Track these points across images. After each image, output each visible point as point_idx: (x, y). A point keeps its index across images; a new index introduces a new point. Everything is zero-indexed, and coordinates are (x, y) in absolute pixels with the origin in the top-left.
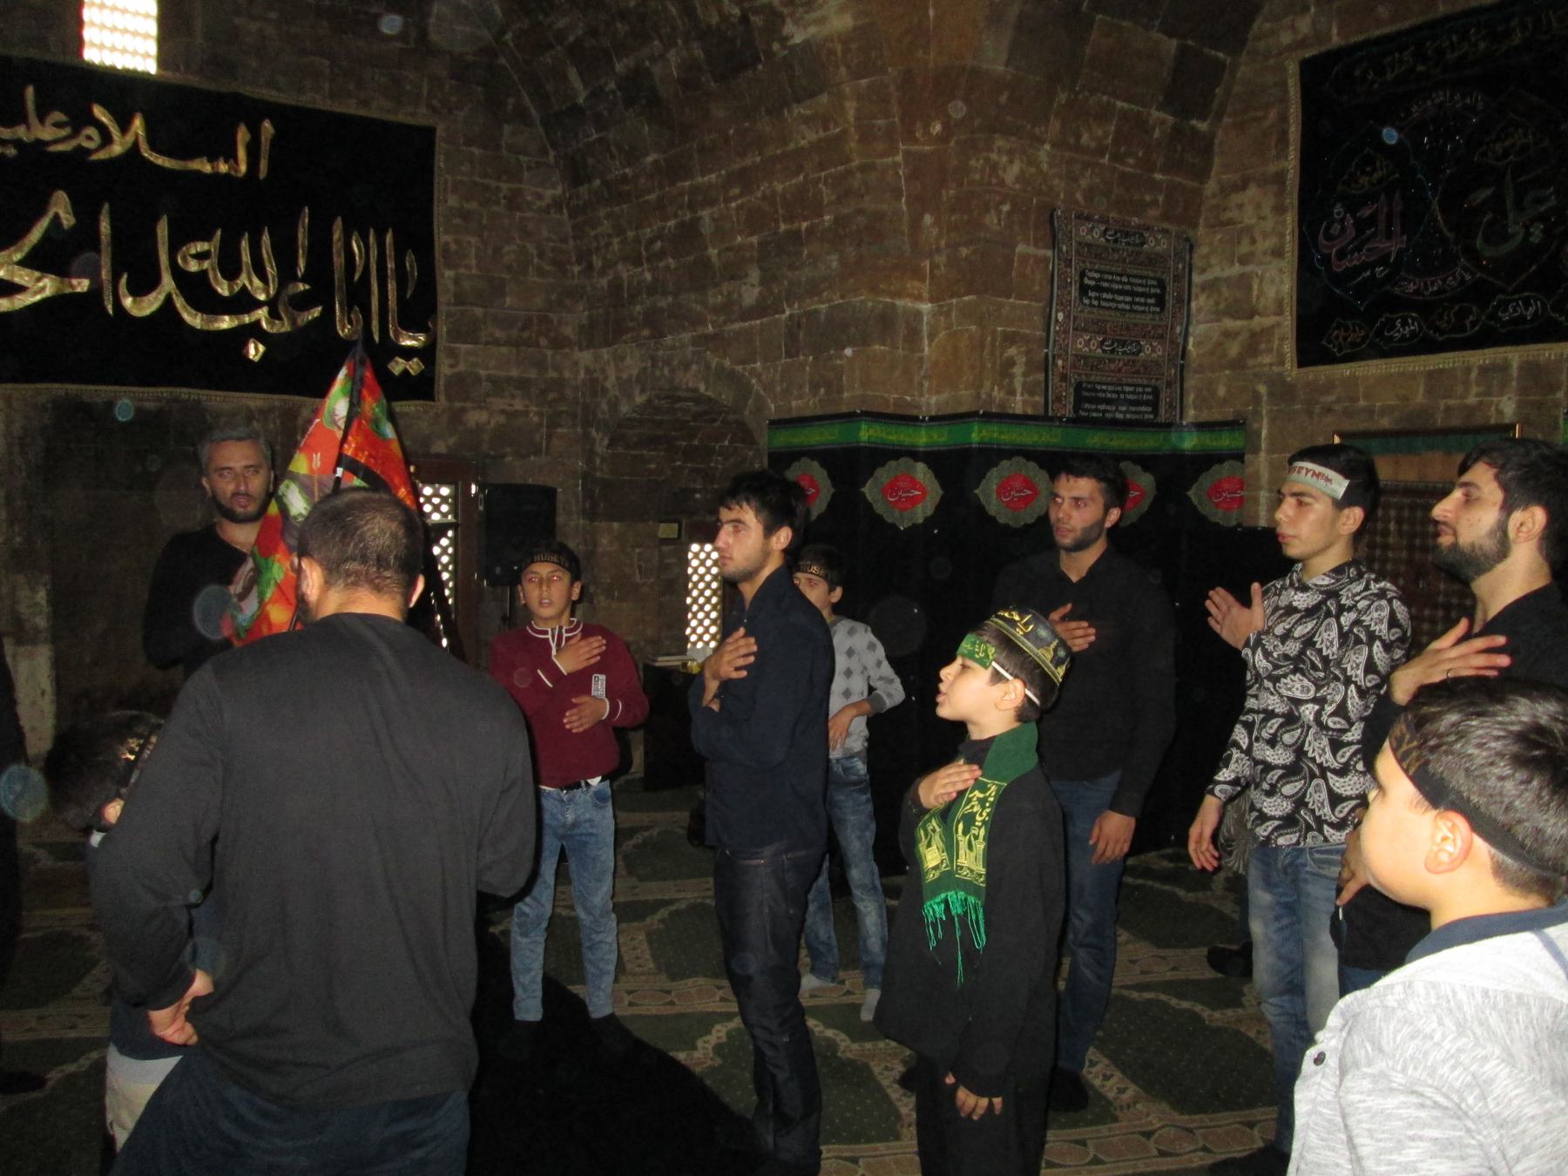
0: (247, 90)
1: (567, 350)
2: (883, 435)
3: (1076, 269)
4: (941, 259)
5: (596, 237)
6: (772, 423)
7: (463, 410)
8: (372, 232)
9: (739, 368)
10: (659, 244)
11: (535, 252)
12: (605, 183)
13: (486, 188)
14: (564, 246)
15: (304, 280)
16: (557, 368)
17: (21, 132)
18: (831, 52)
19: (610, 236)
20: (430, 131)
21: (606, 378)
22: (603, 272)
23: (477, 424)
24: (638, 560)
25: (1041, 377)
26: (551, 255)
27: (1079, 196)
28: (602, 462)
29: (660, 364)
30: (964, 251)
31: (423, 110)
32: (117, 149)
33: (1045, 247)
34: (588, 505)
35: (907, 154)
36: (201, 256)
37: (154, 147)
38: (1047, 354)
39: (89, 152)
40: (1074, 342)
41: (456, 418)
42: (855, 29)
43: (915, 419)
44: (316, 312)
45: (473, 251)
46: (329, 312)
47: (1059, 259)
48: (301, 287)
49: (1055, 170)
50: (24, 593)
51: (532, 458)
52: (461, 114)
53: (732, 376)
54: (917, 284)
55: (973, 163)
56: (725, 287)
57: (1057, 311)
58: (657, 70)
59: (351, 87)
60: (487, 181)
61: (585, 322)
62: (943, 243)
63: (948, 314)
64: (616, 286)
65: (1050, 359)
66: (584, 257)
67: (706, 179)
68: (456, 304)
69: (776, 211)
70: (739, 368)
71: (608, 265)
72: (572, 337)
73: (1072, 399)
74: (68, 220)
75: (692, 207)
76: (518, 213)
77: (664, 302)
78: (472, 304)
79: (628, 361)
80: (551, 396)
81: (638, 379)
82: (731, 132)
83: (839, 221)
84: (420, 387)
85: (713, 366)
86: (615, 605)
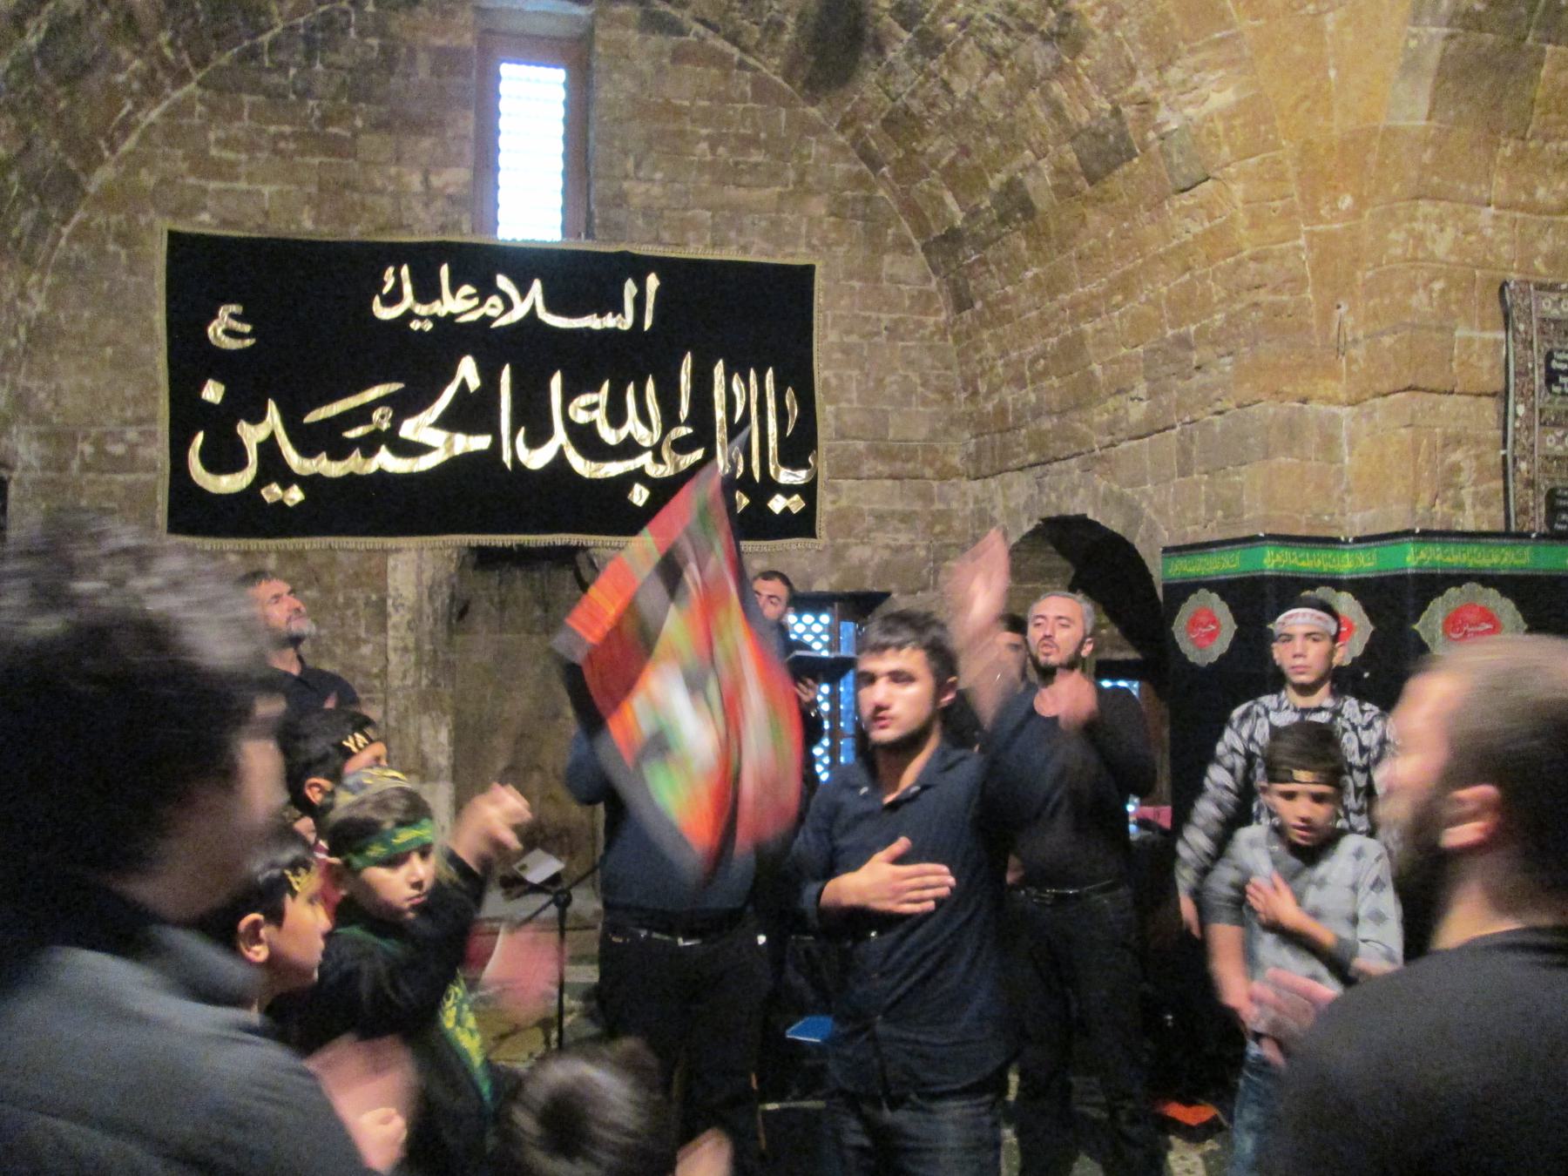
1: (954, 480)
2: (1295, 561)
3: (1539, 351)
4: (1357, 352)
5: (980, 362)
6: (1166, 550)
7: (846, 546)
8: (752, 373)
9: (1128, 491)
10: (1042, 362)
11: (918, 381)
12: (987, 305)
13: (867, 319)
14: (949, 373)
15: (688, 423)
18: (1211, 133)
19: (994, 359)
20: (808, 271)
21: (994, 508)
22: (987, 397)
23: (860, 560)
25: (1499, 484)
26: (935, 383)
27: (1538, 263)
29: (1047, 490)
30: (1387, 341)
31: (803, 249)
32: (520, 311)
33: (1494, 328)
35: (1312, 234)
36: (593, 407)
37: (551, 307)
38: (1504, 457)
39: (493, 319)
40: (1542, 441)
41: (838, 555)
42: (1238, 103)
43: (1336, 541)
44: (698, 454)
45: (854, 384)
47: (1514, 340)
48: (684, 431)
49: (1505, 235)
51: (919, 594)
52: (840, 250)
53: (1121, 500)
54: (1333, 384)
55: (1393, 236)
56: (1111, 403)
57: (1516, 403)
58: (1030, 181)
59: (733, 234)
60: (867, 314)
61: (972, 448)
62: (1360, 334)
63: (1370, 416)
64: (1002, 411)
65: (1510, 461)
66: (970, 384)
67: (1086, 290)
68: (836, 439)
69: (1162, 316)
70: (1128, 491)
71: (993, 389)
72: (959, 466)
73: (1543, 510)
74: (474, 383)
75: (1074, 320)
76: (901, 344)
77: (1047, 424)
78: (855, 438)
79: (1016, 488)
80: (938, 529)
81: (1026, 507)
82: (1110, 235)
83: (1229, 320)
84: (801, 525)
85: (1102, 489)
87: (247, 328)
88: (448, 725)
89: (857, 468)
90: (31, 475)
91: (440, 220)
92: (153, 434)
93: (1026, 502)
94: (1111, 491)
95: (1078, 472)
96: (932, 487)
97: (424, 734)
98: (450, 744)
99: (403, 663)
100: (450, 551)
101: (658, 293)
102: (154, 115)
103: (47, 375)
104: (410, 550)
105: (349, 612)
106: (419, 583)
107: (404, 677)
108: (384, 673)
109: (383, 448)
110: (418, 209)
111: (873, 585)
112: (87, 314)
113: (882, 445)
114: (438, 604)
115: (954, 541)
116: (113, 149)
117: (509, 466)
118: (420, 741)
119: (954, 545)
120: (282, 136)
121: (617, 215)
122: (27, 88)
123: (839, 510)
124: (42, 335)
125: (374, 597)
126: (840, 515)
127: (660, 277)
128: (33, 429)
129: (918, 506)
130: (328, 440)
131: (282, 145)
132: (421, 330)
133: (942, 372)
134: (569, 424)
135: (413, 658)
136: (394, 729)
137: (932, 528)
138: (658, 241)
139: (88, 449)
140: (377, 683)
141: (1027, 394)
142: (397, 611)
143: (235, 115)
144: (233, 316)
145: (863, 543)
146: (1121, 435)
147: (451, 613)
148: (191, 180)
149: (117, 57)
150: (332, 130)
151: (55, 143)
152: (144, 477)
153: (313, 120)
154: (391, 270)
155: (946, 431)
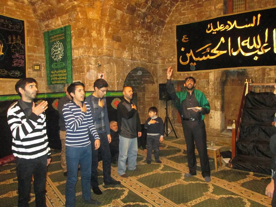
0: (255, 10)
15: (267, 43)
17: (217, 30)
32: (232, 27)
37: (238, 25)
39: (227, 29)
44: (270, 49)
48: (265, 45)
50: (216, 103)
74: (224, 41)
87: (187, 38)
90: (161, 64)
91: (217, 14)
92: (175, 57)
97: (216, 103)
101: (260, 17)
102: (174, 8)
103: (162, 51)
104: (213, 72)
106: (214, 77)
107: (212, 93)
108: (209, 93)
109: (208, 55)
110: (214, 12)
112: (166, 40)
114: (218, 81)
116: (169, 15)
118: (215, 104)
120: (192, 6)
121: (252, 4)
122: (151, 11)
124: (161, 44)
125: (207, 80)
127: (261, 14)
128: (160, 58)
130: (199, 55)
131: (192, 8)
132: (214, 34)
134: (241, 46)
135: (213, 90)
138: (261, 7)
139: (167, 60)
140: (208, 94)
142: (211, 82)
143: (185, 5)
144: (185, 37)
147: (220, 82)
148: (179, 17)
149: (165, 2)
150: (200, 3)
151: (158, 17)
152: (175, 63)
153: (196, 2)
154: (209, 24)
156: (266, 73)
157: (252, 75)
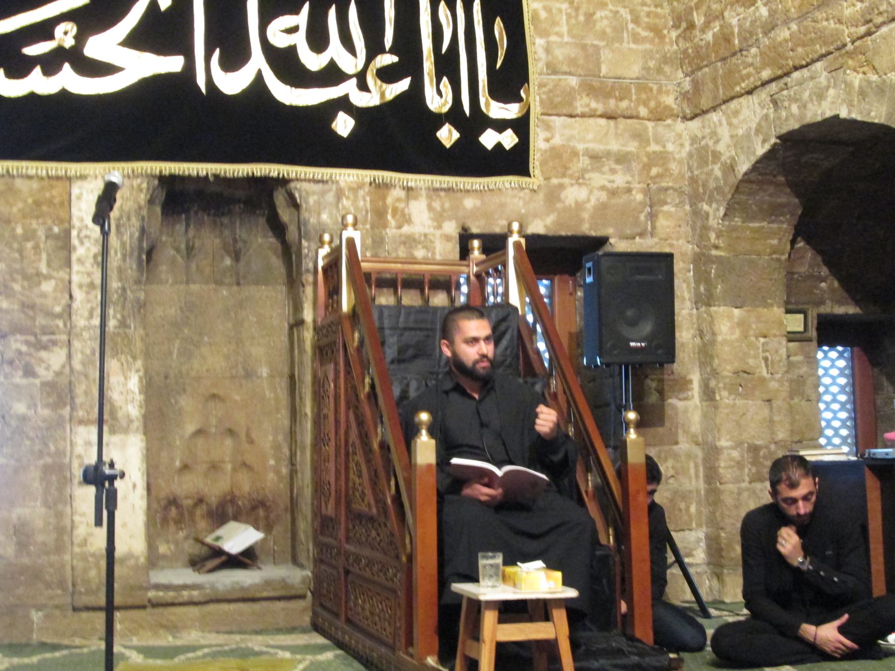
1: (669, 121)
7: (561, 187)
11: (629, 18)
14: (659, 10)
15: (392, 51)
16: (658, 141)
21: (717, 142)
22: (707, 25)
23: (577, 203)
24: (764, 351)
26: (646, 20)
28: (718, 237)
34: (702, 289)
36: (293, 30)
41: (553, 196)
44: (404, 85)
45: (564, 17)
46: (417, 88)
64: (725, 37)
72: (675, 106)
78: (566, 73)
79: (745, 113)
80: (654, 171)
81: (758, 131)
86: (740, 402)
88: (138, 371)
89: (571, 104)
93: (759, 125)
94: (869, 82)
95: (825, 73)
96: (647, 128)
98: (140, 393)
99: (89, 301)
100: (139, 181)
105: (29, 245)
108: (68, 311)
111: (590, 229)
113: (596, 84)
114: (126, 238)
115: (670, 184)
117: (204, 90)
119: (672, 188)
123: (552, 149)
126: (555, 154)
129: (632, 147)
133: (653, 9)
136: (79, 373)
137: (650, 169)
141: (757, 8)
142: (82, 243)
145: (580, 185)
146: (879, 20)
147: (141, 248)
155: (659, 71)
156: (390, 211)
157: (325, 217)
